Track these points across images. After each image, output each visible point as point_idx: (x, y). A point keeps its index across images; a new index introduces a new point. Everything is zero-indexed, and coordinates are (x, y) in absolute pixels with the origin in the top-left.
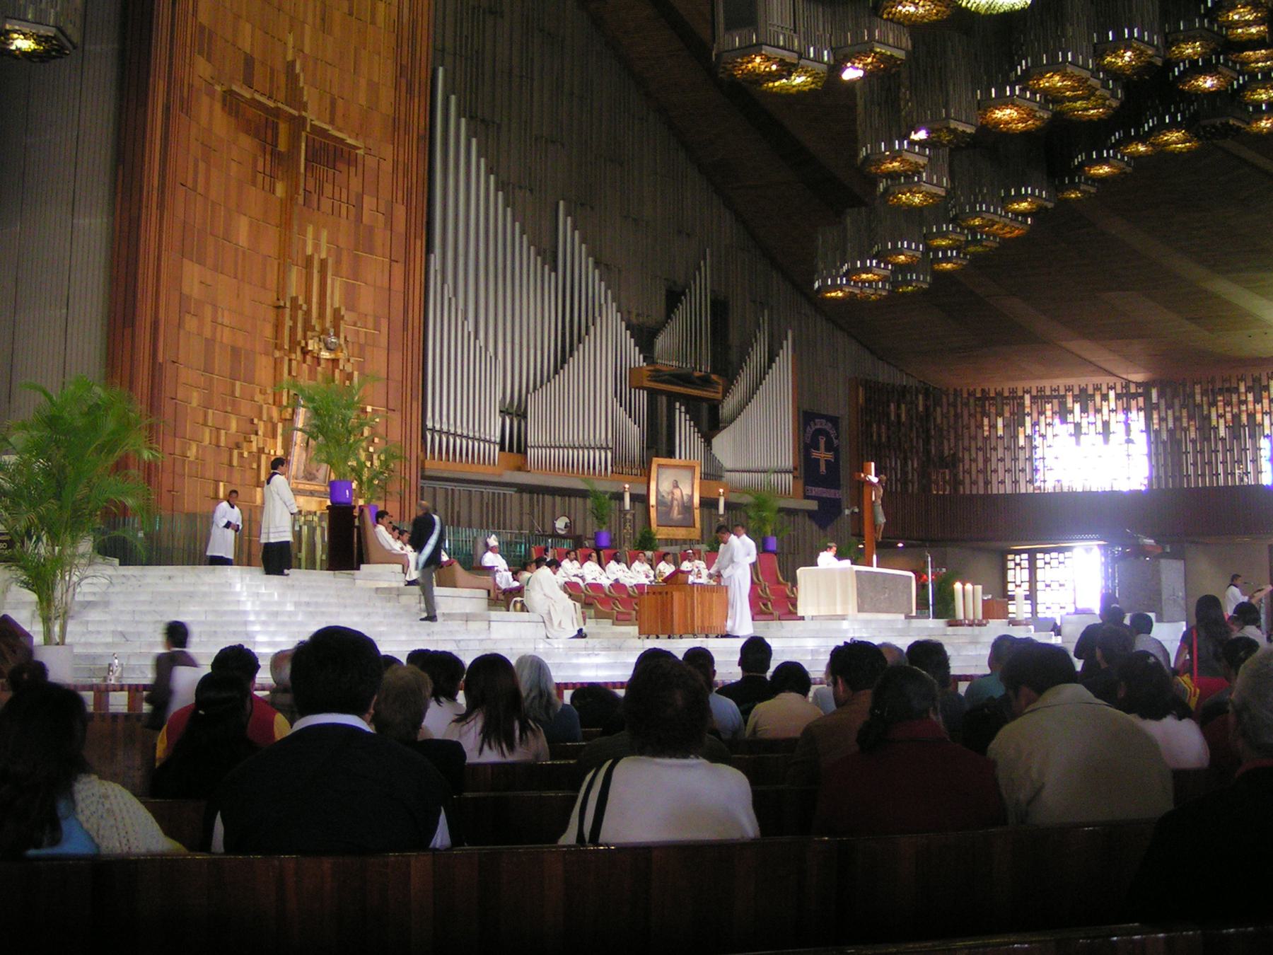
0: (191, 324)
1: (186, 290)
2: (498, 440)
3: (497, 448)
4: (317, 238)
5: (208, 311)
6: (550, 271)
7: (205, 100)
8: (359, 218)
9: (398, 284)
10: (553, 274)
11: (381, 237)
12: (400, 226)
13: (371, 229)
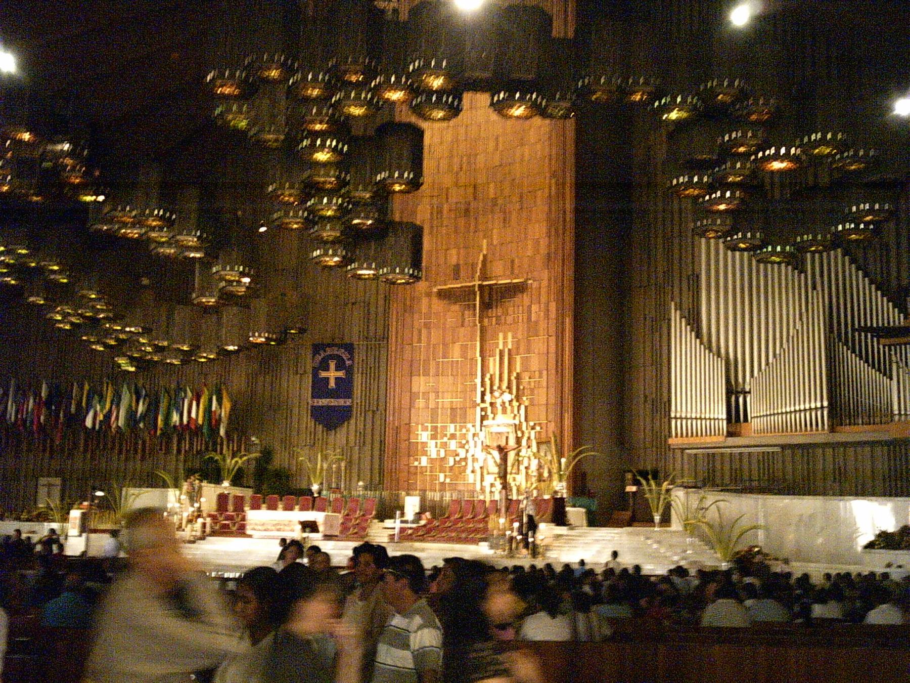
0: (420, 403)
1: (415, 389)
2: (724, 416)
3: (725, 422)
4: (505, 338)
5: (432, 396)
6: (800, 272)
7: (425, 301)
8: (529, 318)
9: (553, 349)
10: (803, 275)
11: (542, 325)
12: (553, 315)
13: (537, 322)
